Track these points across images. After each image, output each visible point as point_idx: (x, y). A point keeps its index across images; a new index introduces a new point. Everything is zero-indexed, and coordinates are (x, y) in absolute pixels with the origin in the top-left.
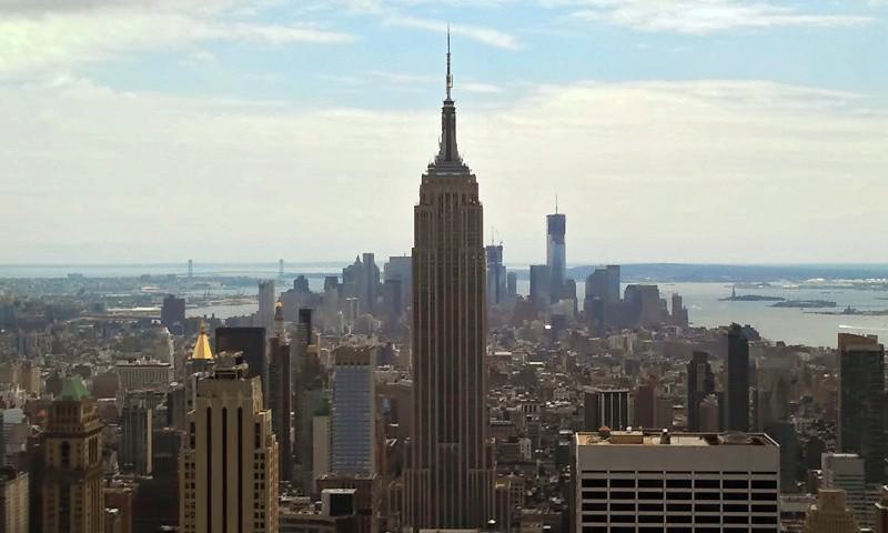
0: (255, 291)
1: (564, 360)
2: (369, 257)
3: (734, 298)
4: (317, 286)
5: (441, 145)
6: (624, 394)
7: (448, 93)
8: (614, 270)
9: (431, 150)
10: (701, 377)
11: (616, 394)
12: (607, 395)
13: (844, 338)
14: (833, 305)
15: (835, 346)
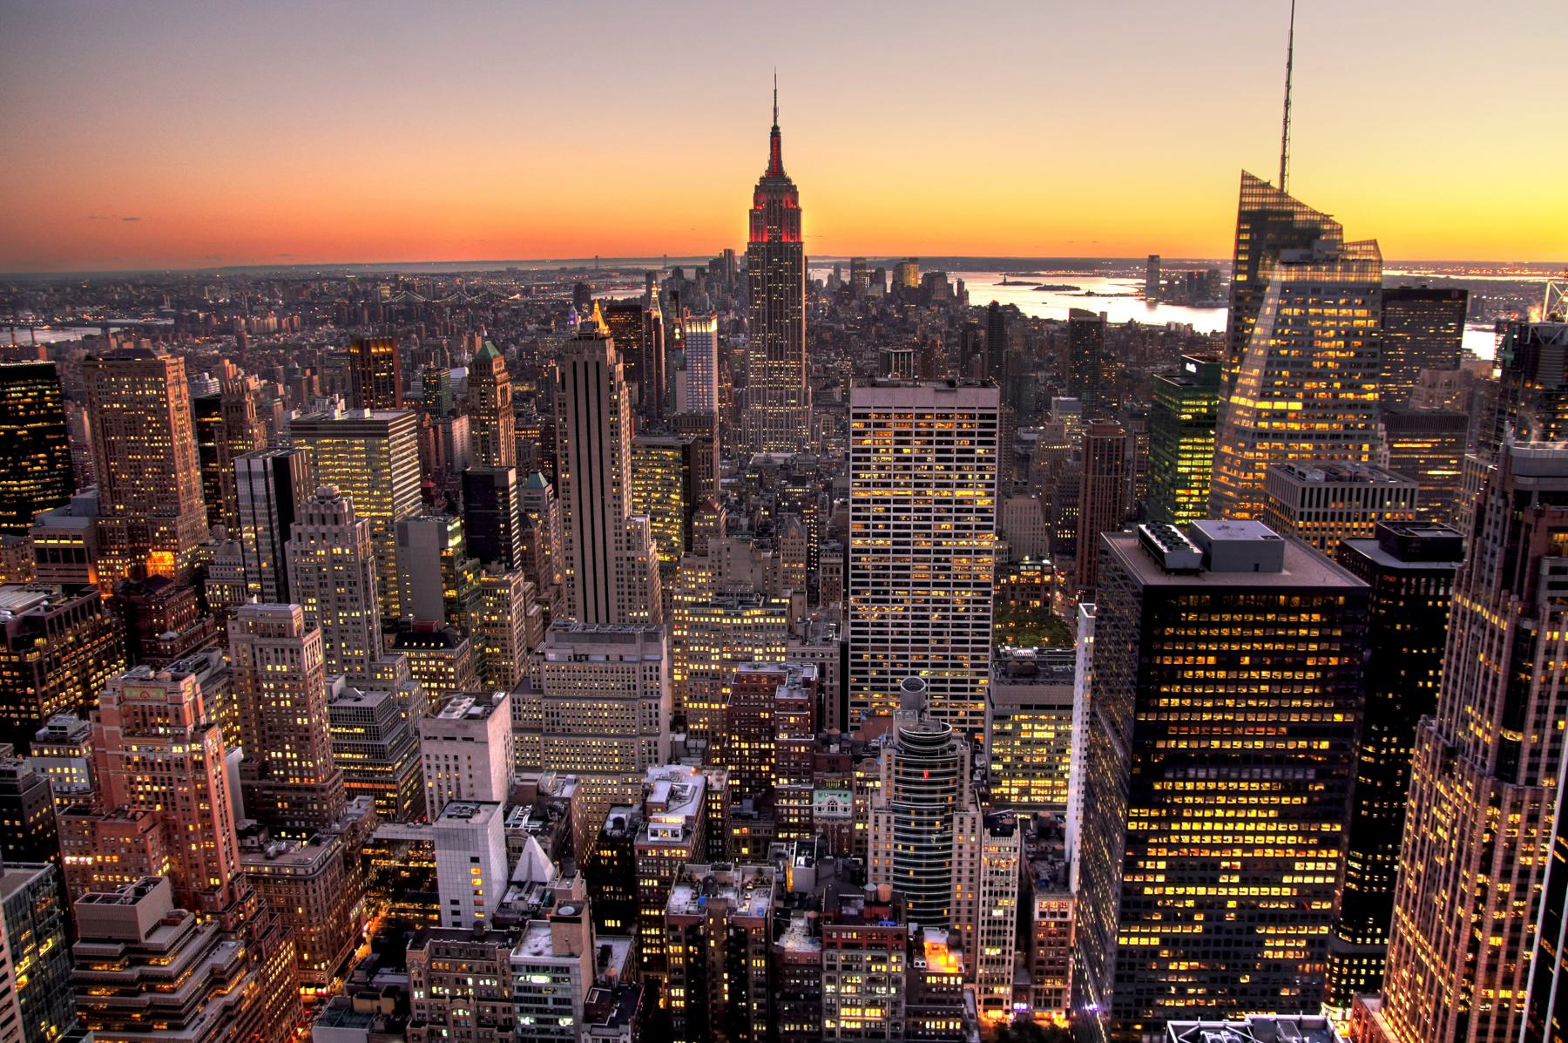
0: (643, 279)
1: (873, 330)
2: (729, 253)
3: (1005, 283)
4: (690, 275)
5: (770, 162)
6: (909, 354)
7: (775, 121)
8: (914, 260)
9: (762, 166)
10: (970, 341)
11: (903, 354)
12: (896, 354)
13: (1073, 312)
14: (1078, 289)
15: (1066, 317)
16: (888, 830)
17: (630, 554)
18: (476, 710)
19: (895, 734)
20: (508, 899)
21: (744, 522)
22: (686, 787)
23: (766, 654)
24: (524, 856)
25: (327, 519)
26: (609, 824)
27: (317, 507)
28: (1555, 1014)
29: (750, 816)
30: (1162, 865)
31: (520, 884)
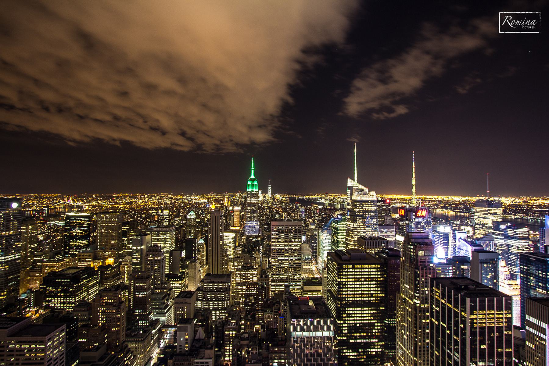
16: (283, 322)
17: (223, 258)
18: (188, 296)
19: (284, 298)
20: (193, 344)
21: (246, 250)
22: (236, 313)
23: (253, 280)
24: (198, 332)
25: (155, 251)
26: (218, 323)
27: (153, 248)
28: (505, 357)
29: (250, 319)
30: (346, 328)
31: (197, 340)
